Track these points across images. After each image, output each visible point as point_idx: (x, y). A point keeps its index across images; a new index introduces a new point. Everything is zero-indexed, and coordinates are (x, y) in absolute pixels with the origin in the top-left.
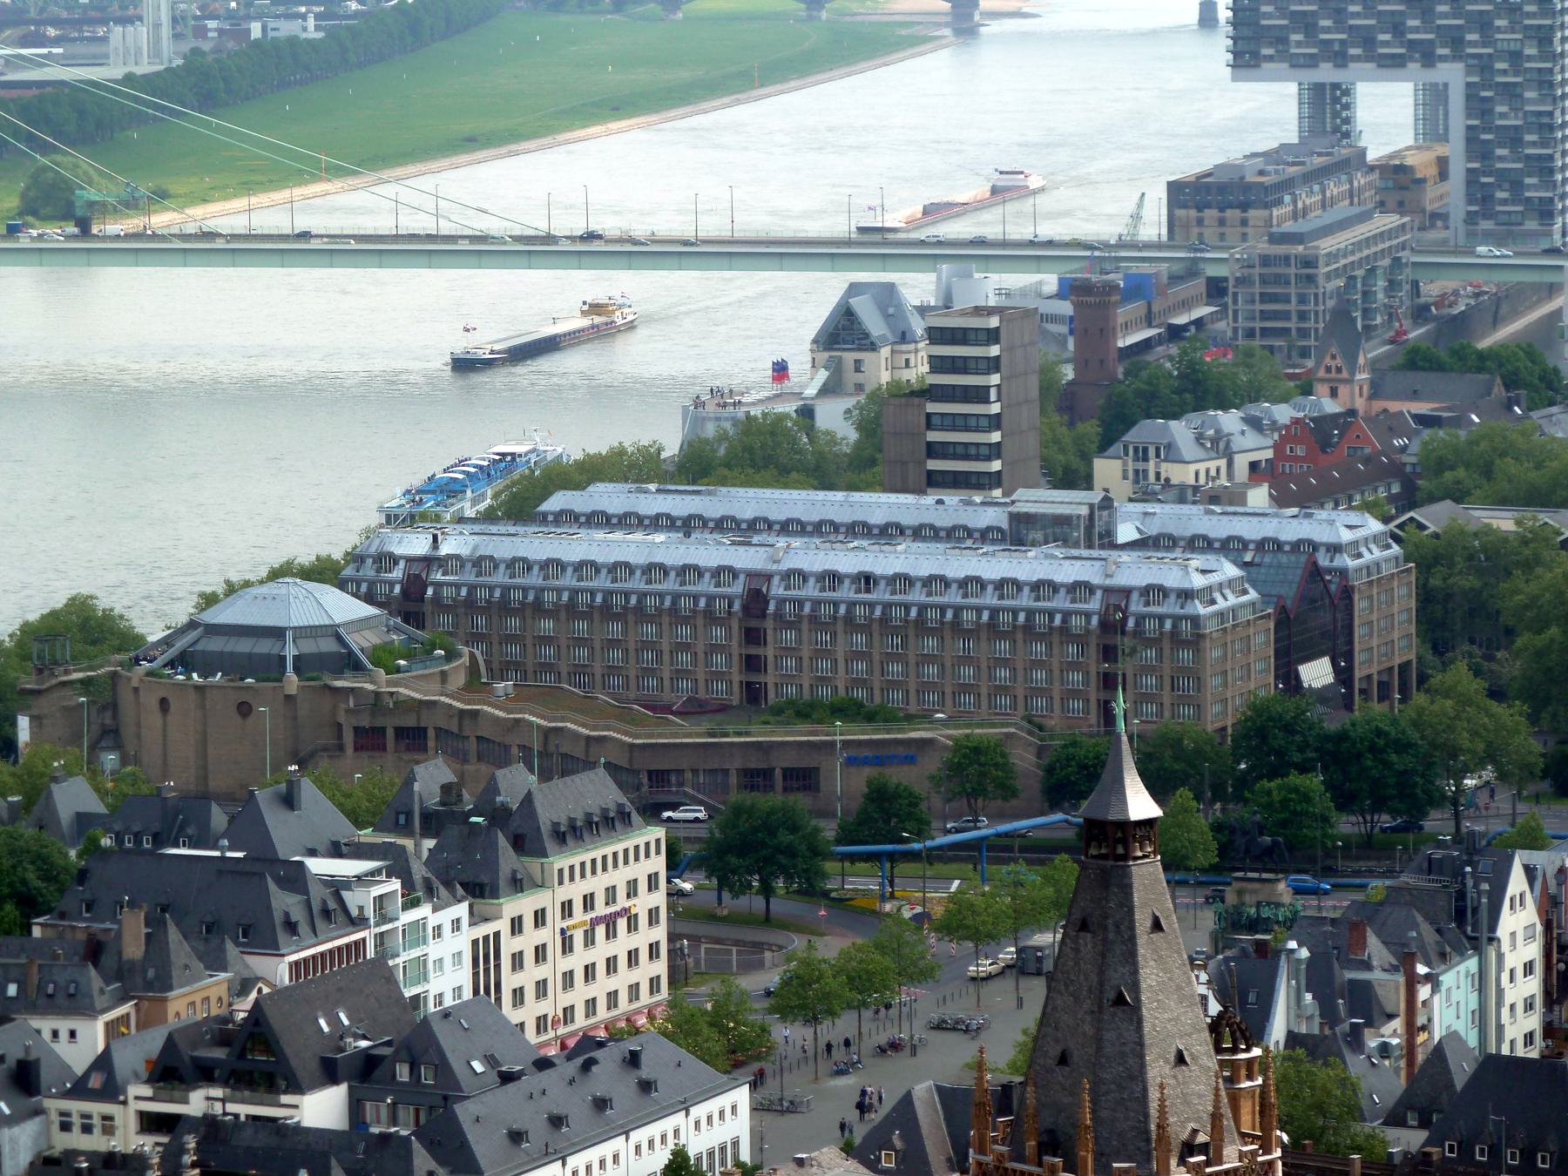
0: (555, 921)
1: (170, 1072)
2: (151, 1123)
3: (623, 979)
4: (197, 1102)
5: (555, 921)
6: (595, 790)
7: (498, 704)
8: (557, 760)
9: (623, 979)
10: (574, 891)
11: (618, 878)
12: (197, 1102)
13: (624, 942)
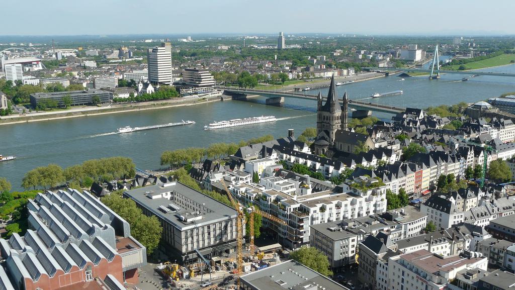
0: (505, 132)
1: (470, 140)
2: (468, 145)
3: (510, 138)
4: (472, 144)
5: (505, 132)
6: (510, 121)
7: (501, 113)
8: (506, 118)
9: (510, 138)
10: (507, 130)
11: (511, 129)
12: (472, 144)
13: (511, 134)
